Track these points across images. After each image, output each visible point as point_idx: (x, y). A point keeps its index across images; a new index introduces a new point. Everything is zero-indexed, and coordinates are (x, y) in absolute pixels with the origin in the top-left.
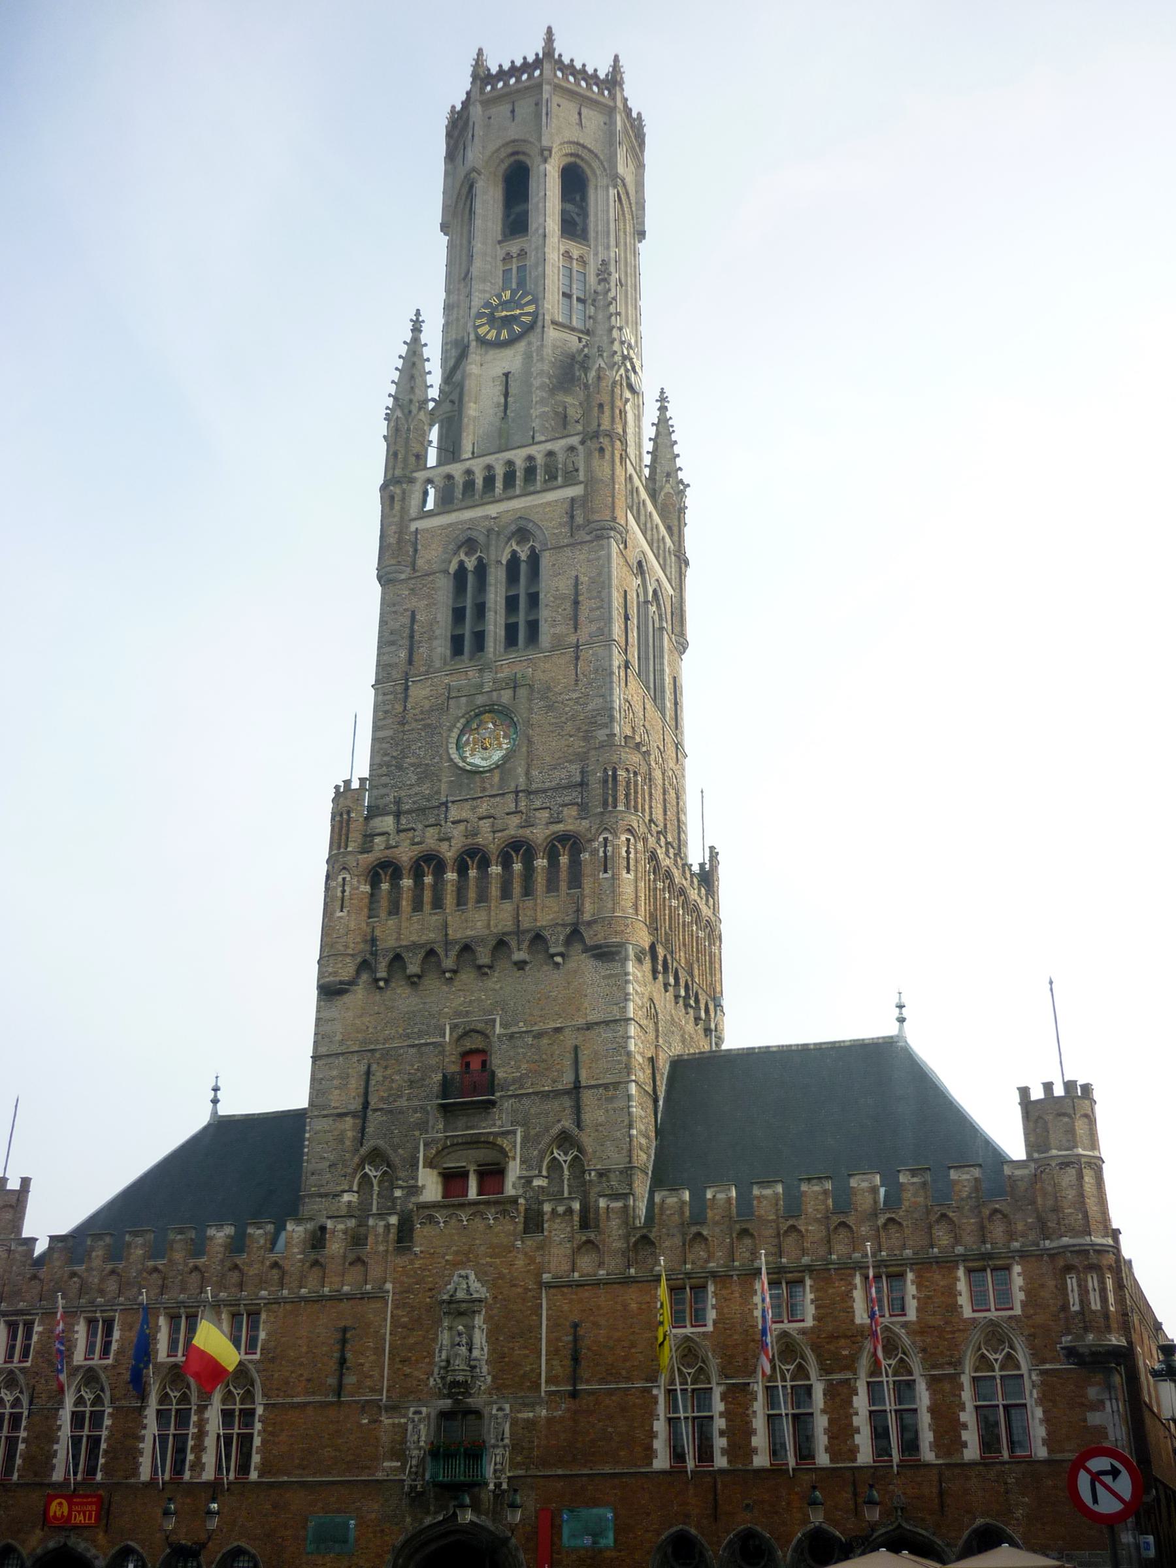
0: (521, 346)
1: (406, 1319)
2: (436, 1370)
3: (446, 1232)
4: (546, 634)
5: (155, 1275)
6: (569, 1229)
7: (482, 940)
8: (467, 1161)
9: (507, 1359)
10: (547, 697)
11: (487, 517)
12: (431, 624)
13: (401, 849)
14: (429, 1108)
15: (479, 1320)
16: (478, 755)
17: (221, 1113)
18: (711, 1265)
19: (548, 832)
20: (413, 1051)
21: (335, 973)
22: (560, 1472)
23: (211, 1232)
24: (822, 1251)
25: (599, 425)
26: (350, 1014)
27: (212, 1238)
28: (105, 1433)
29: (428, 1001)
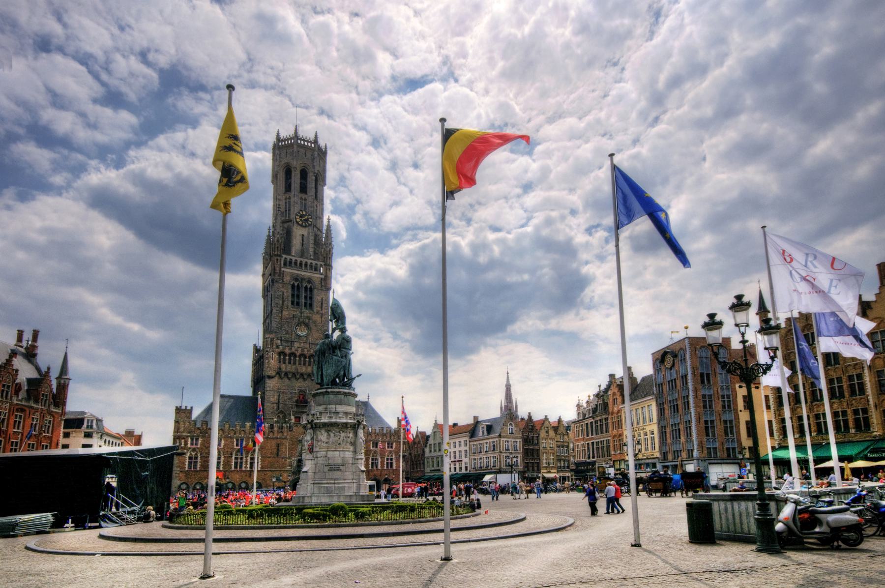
0: (307, 229)
7: (306, 374)
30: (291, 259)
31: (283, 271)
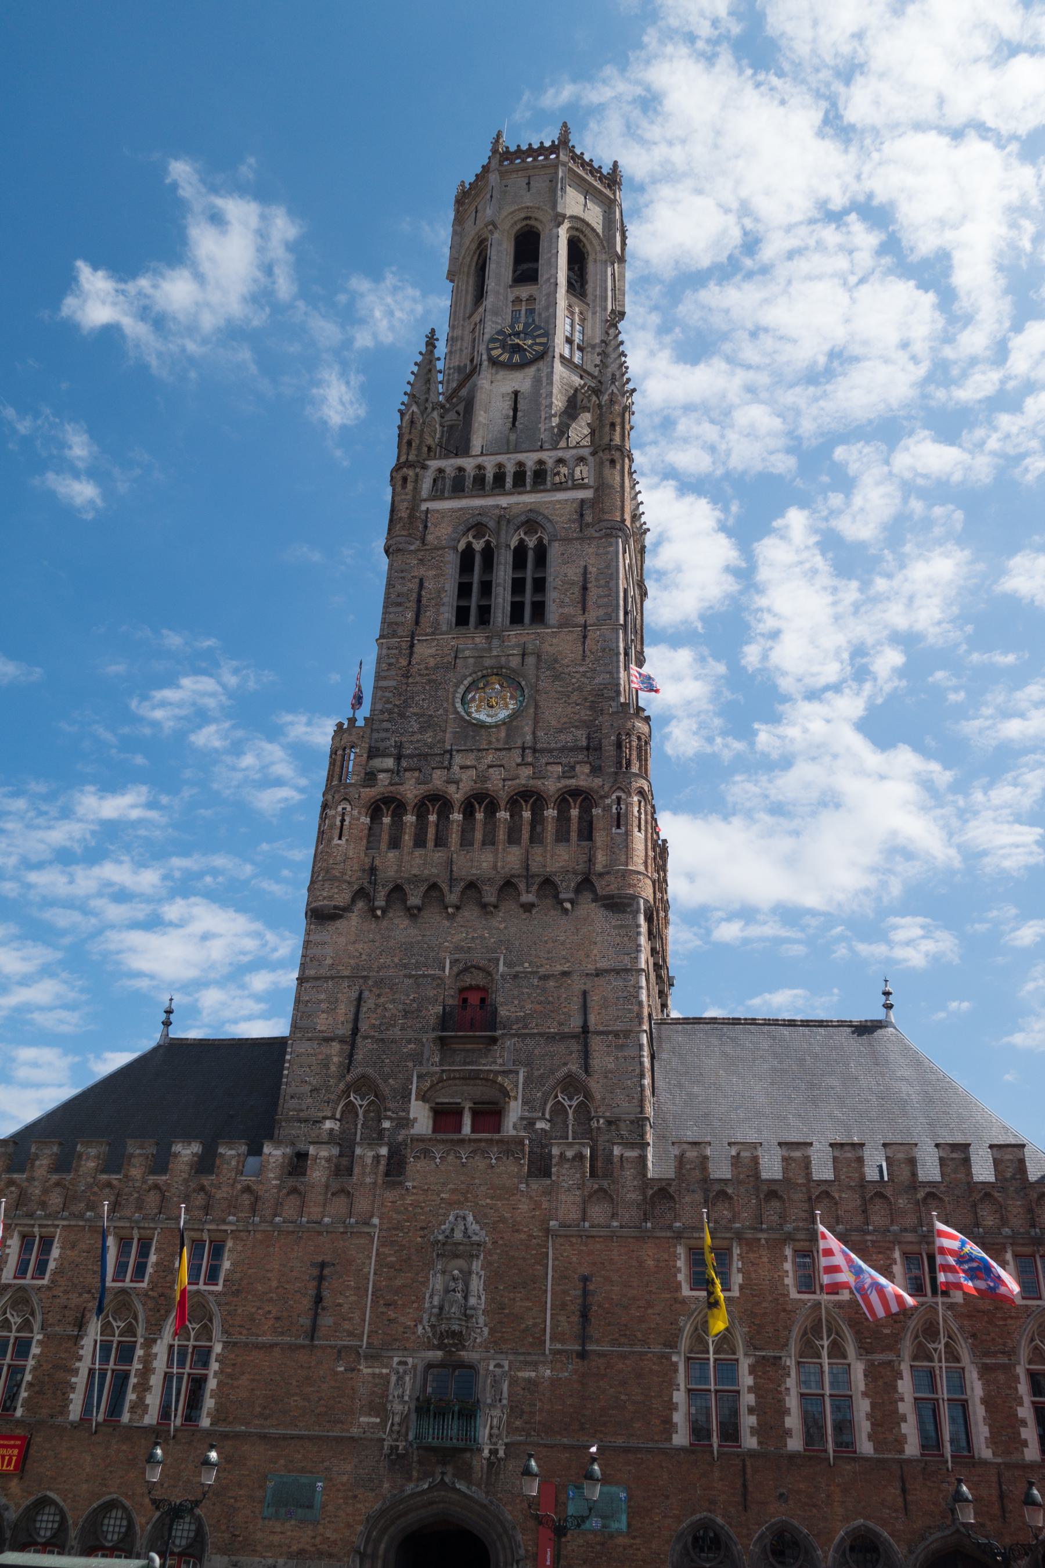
0: (531, 371)
1: (393, 1259)
2: (426, 1316)
3: (442, 1168)
4: (553, 613)
5: (107, 1190)
6: (578, 1176)
8: (464, 1097)
9: (507, 1311)
10: (554, 668)
11: (497, 506)
12: (439, 592)
13: (406, 786)
14: (424, 1040)
15: (476, 1265)
16: (484, 712)
17: (171, 1036)
18: (737, 1225)
19: (560, 785)
20: (407, 981)
21: (330, 898)
22: (565, 1441)
23: (177, 1148)
24: (858, 1220)
25: (611, 440)
26: (342, 940)
27: (177, 1155)
28: (31, 1363)
29: (428, 933)
30: (461, 469)
31: (427, 511)
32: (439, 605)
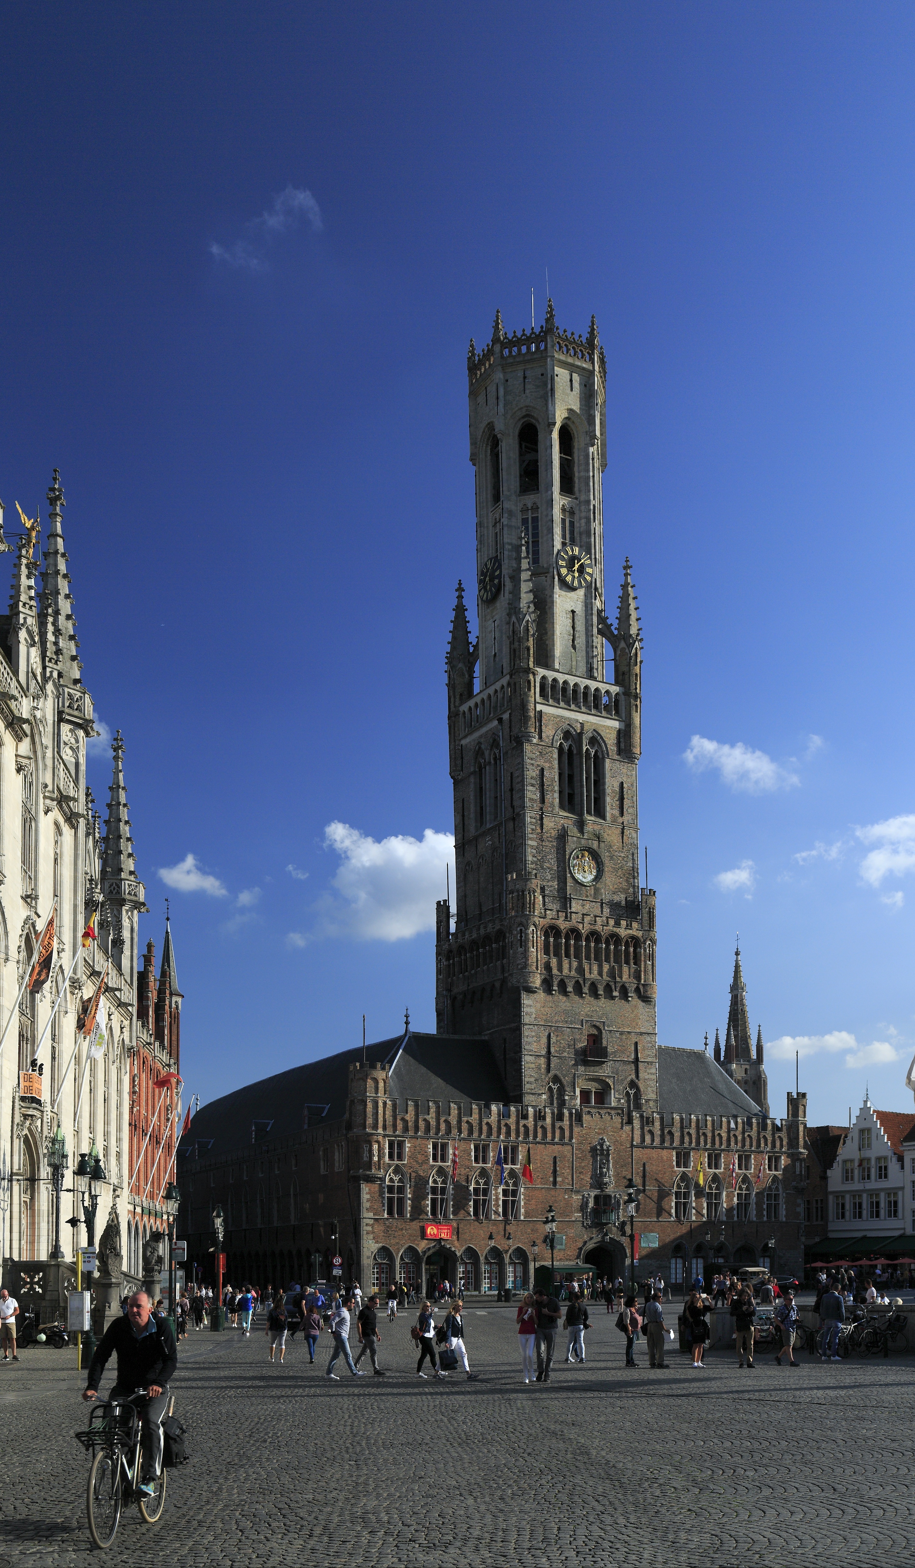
8: (593, 1087)
11: (577, 721)
26: (538, 1005)
32: (553, 791)
